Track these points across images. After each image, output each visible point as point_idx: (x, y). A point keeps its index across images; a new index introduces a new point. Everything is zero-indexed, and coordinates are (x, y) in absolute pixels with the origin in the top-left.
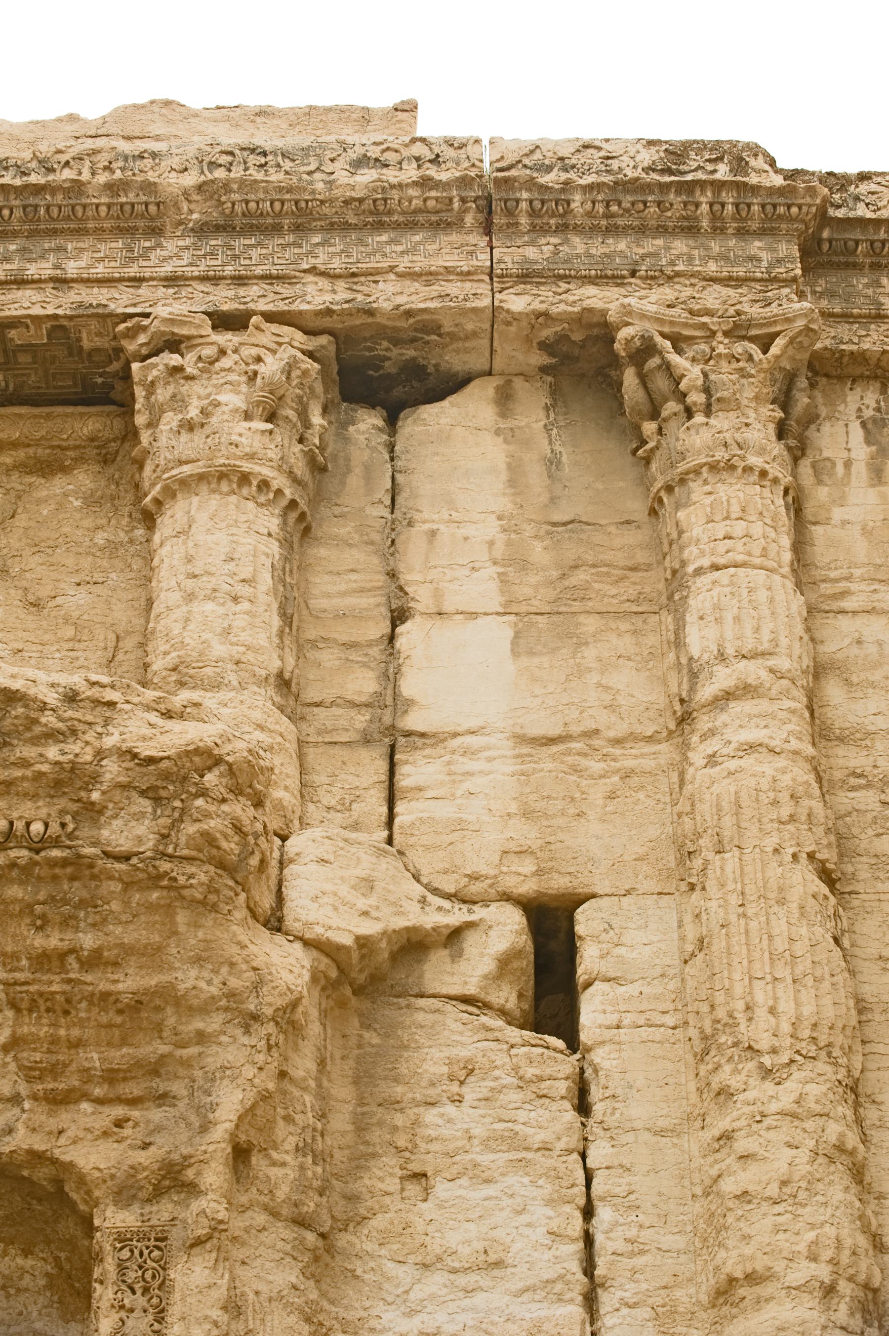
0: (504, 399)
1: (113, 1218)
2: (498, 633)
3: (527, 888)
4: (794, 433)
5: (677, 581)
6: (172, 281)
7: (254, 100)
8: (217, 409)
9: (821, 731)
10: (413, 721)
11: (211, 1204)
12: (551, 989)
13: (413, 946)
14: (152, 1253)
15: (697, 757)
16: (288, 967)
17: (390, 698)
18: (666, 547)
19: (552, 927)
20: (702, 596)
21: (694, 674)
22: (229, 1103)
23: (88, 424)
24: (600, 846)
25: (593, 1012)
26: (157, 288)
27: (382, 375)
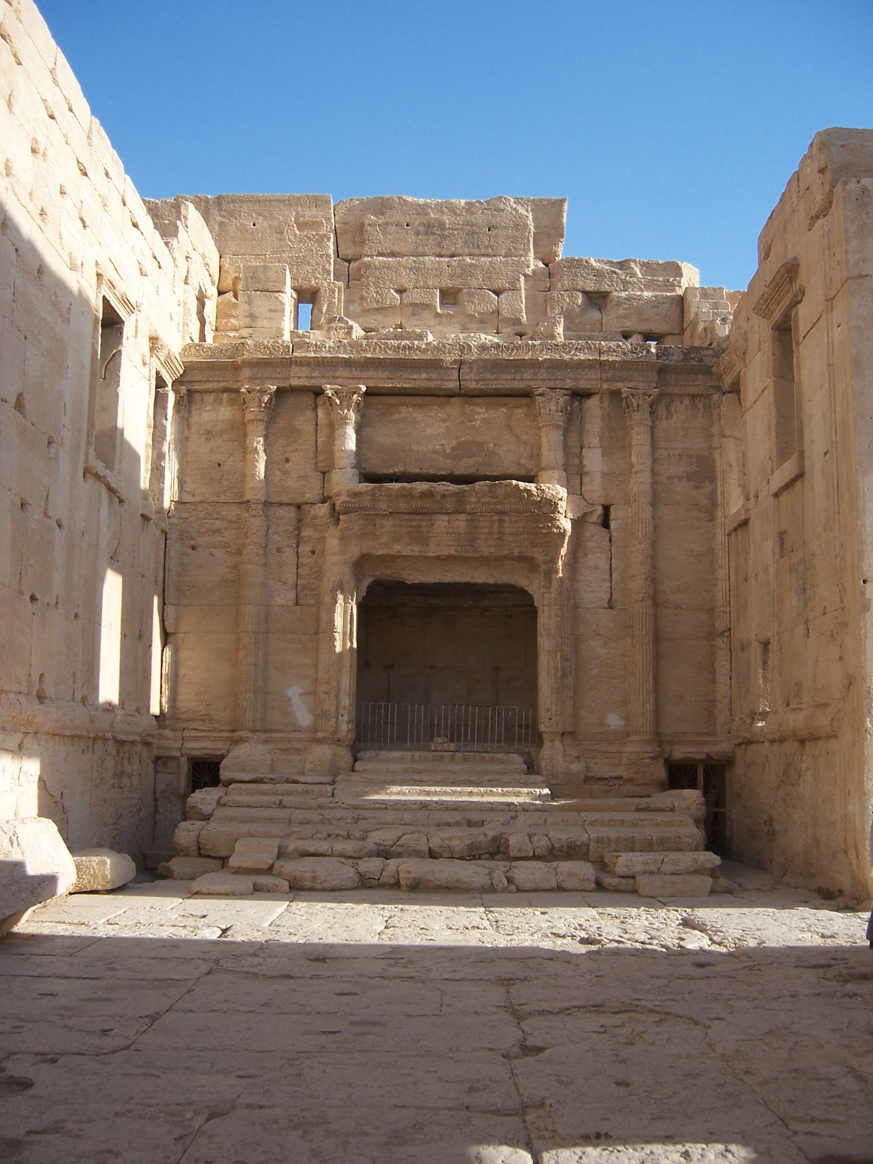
0: (601, 399)
1: (543, 567)
3: (603, 503)
4: (652, 413)
6: (543, 380)
9: (654, 473)
10: (586, 470)
12: (605, 523)
13: (585, 514)
15: (633, 480)
17: (581, 465)
19: (606, 509)
20: (635, 450)
21: (632, 466)
23: (525, 401)
25: (613, 525)
27: (579, 395)
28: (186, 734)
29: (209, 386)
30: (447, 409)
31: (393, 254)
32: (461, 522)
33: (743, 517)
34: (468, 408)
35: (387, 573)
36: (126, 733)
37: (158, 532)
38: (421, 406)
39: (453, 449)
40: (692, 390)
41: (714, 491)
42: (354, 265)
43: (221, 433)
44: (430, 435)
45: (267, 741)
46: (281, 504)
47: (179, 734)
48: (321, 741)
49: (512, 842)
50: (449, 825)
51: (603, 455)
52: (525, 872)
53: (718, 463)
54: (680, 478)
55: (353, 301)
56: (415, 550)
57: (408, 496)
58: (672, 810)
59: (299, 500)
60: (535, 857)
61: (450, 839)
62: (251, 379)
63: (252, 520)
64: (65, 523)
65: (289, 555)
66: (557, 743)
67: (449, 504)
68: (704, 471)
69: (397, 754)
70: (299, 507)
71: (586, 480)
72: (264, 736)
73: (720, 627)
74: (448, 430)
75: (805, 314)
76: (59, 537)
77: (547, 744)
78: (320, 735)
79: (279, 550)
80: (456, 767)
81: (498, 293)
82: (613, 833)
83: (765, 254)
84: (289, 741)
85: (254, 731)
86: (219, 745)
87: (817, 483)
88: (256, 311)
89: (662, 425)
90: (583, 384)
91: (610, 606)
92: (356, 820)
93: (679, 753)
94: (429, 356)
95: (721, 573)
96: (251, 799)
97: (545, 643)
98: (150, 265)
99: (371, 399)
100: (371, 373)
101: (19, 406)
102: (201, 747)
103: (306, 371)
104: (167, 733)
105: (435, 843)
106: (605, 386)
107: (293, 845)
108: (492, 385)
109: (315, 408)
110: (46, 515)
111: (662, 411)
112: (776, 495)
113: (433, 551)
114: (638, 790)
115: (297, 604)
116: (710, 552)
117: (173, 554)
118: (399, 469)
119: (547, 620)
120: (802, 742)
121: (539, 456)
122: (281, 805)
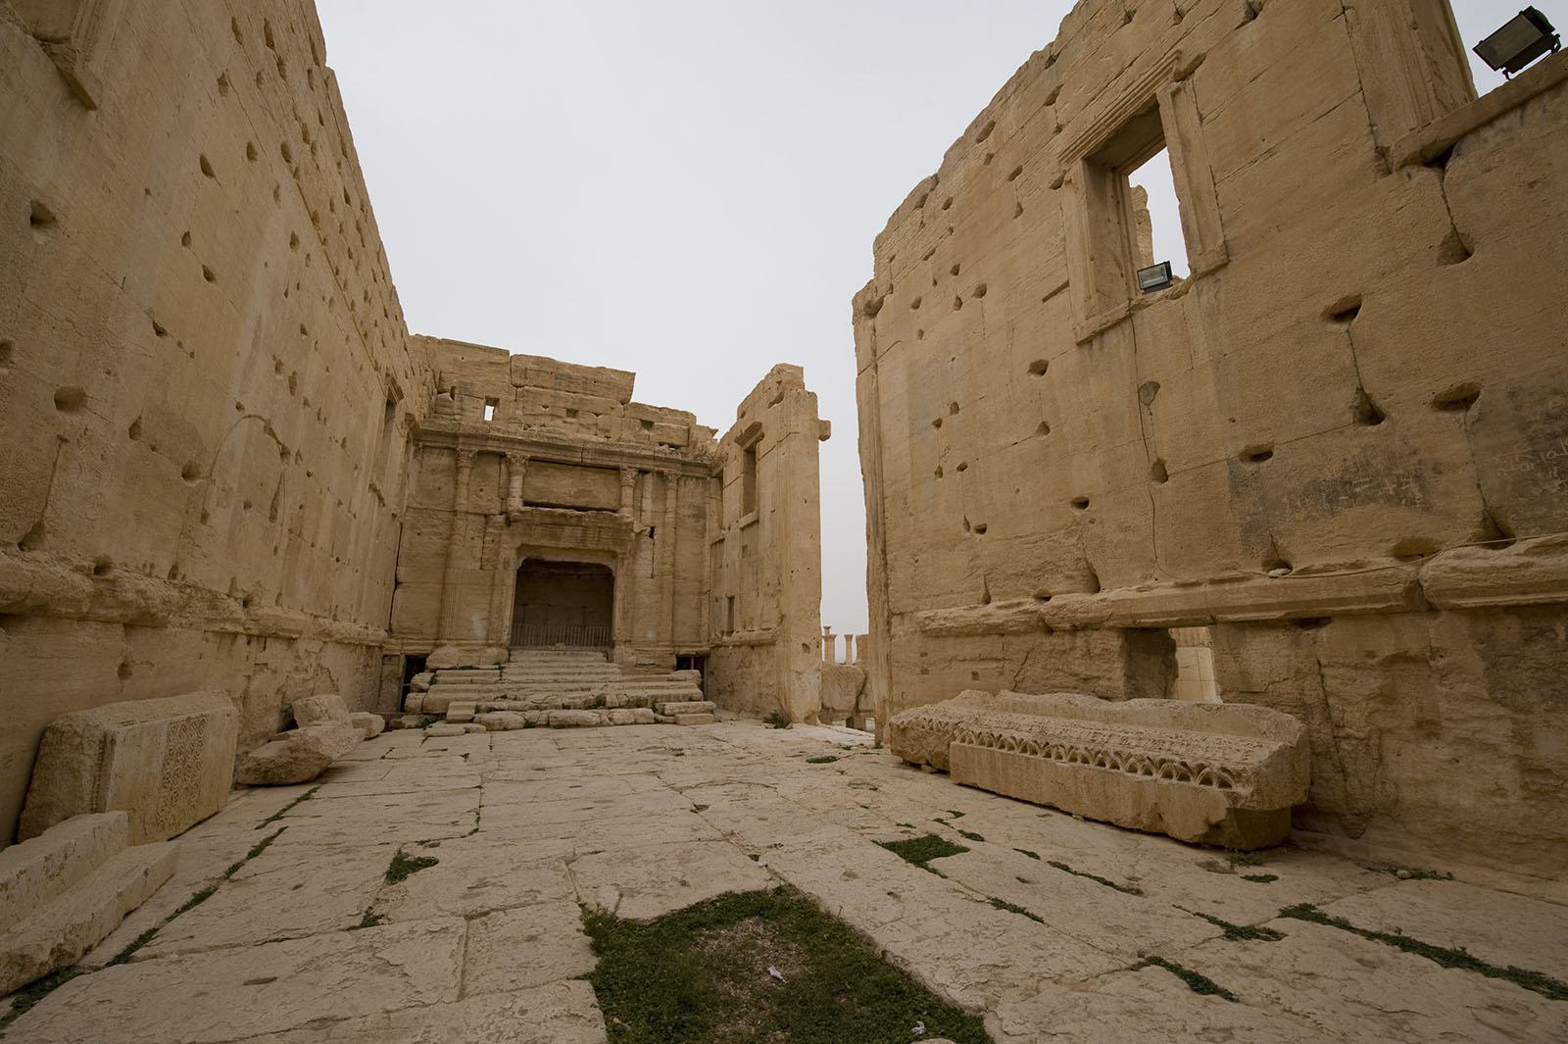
2: (650, 501)
4: (678, 484)
5: (666, 499)
7: (615, 368)
8: (629, 477)
9: (676, 513)
11: (627, 556)
12: (651, 536)
14: (622, 559)
16: (633, 535)
17: (641, 507)
18: (666, 494)
19: (653, 529)
20: (668, 501)
22: (629, 547)
24: (658, 522)
25: (655, 537)
26: (623, 464)
27: (643, 472)
28: (405, 641)
29: (437, 444)
30: (573, 472)
31: (543, 387)
32: (579, 532)
33: (722, 537)
34: (584, 473)
35: (534, 555)
36: (373, 641)
37: (398, 524)
38: (560, 469)
39: (575, 493)
40: (697, 475)
41: (705, 524)
42: (519, 389)
43: (442, 471)
44: (563, 487)
45: (457, 645)
46: (476, 514)
47: (400, 641)
48: (489, 646)
49: (608, 699)
50: (571, 690)
51: (653, 502)
52: (619, 714)
53: (707, 510)
54: (689, 516)
55: (518, 409)
56: (552, 544)
57: (552, 515)
58: (685, 680)
59: (487, 512)
60: (620, 707)
61: (573, 698)
62: (464, 444)
63: (459, 521)
64: (357, 516)
65: (479, 542)
66: (623, 647)
67: (573, 521)
68: (700, 514)
69: (534, 652)
70: (486, 516)
71: (643, 514)
72: (456, 642)
73: (705, 590)
74: (572, 482)
75: (762, 447)
76: (354, 522)
77: (617, 647)
78: (490, 642)
79: (473, 539)
80: (568, 659)
81: (597, 415)
82: (659, 692)
83: (742, 415)
84: (471, 645)
85: (450, 639)
86: (426, 648)
87: (766, 523)
88: (466, 407)
89: (682, 490)
90: (645, 467)
91: (652, 577)
92: (519, 690)
93: (683, 651)
94: (566, 444)
95: (707, 563)
96: (453, 679)
97: (618, 595)
98: (409, 372)
99: (533, 462)
100: (534, 449)
101: (343, 445)
102: (414, 649)
103: (496, 443)
104: (393, 641)
105: (566, 701)
106: (656, 469)
107: (484, 705)
108: (599, 462)
109: (500, 464)
110: (349, 512)
111: (682, 483)
112: (742, 529)
113: (562, 544)
114: (663, 670)
115: (481, 569)
116: (702, 553)
117: (405, 538)
118: (545, 500)
119: (620, 583)
120: (752, 647)
121: (620, 500)
122: (471, 682)
